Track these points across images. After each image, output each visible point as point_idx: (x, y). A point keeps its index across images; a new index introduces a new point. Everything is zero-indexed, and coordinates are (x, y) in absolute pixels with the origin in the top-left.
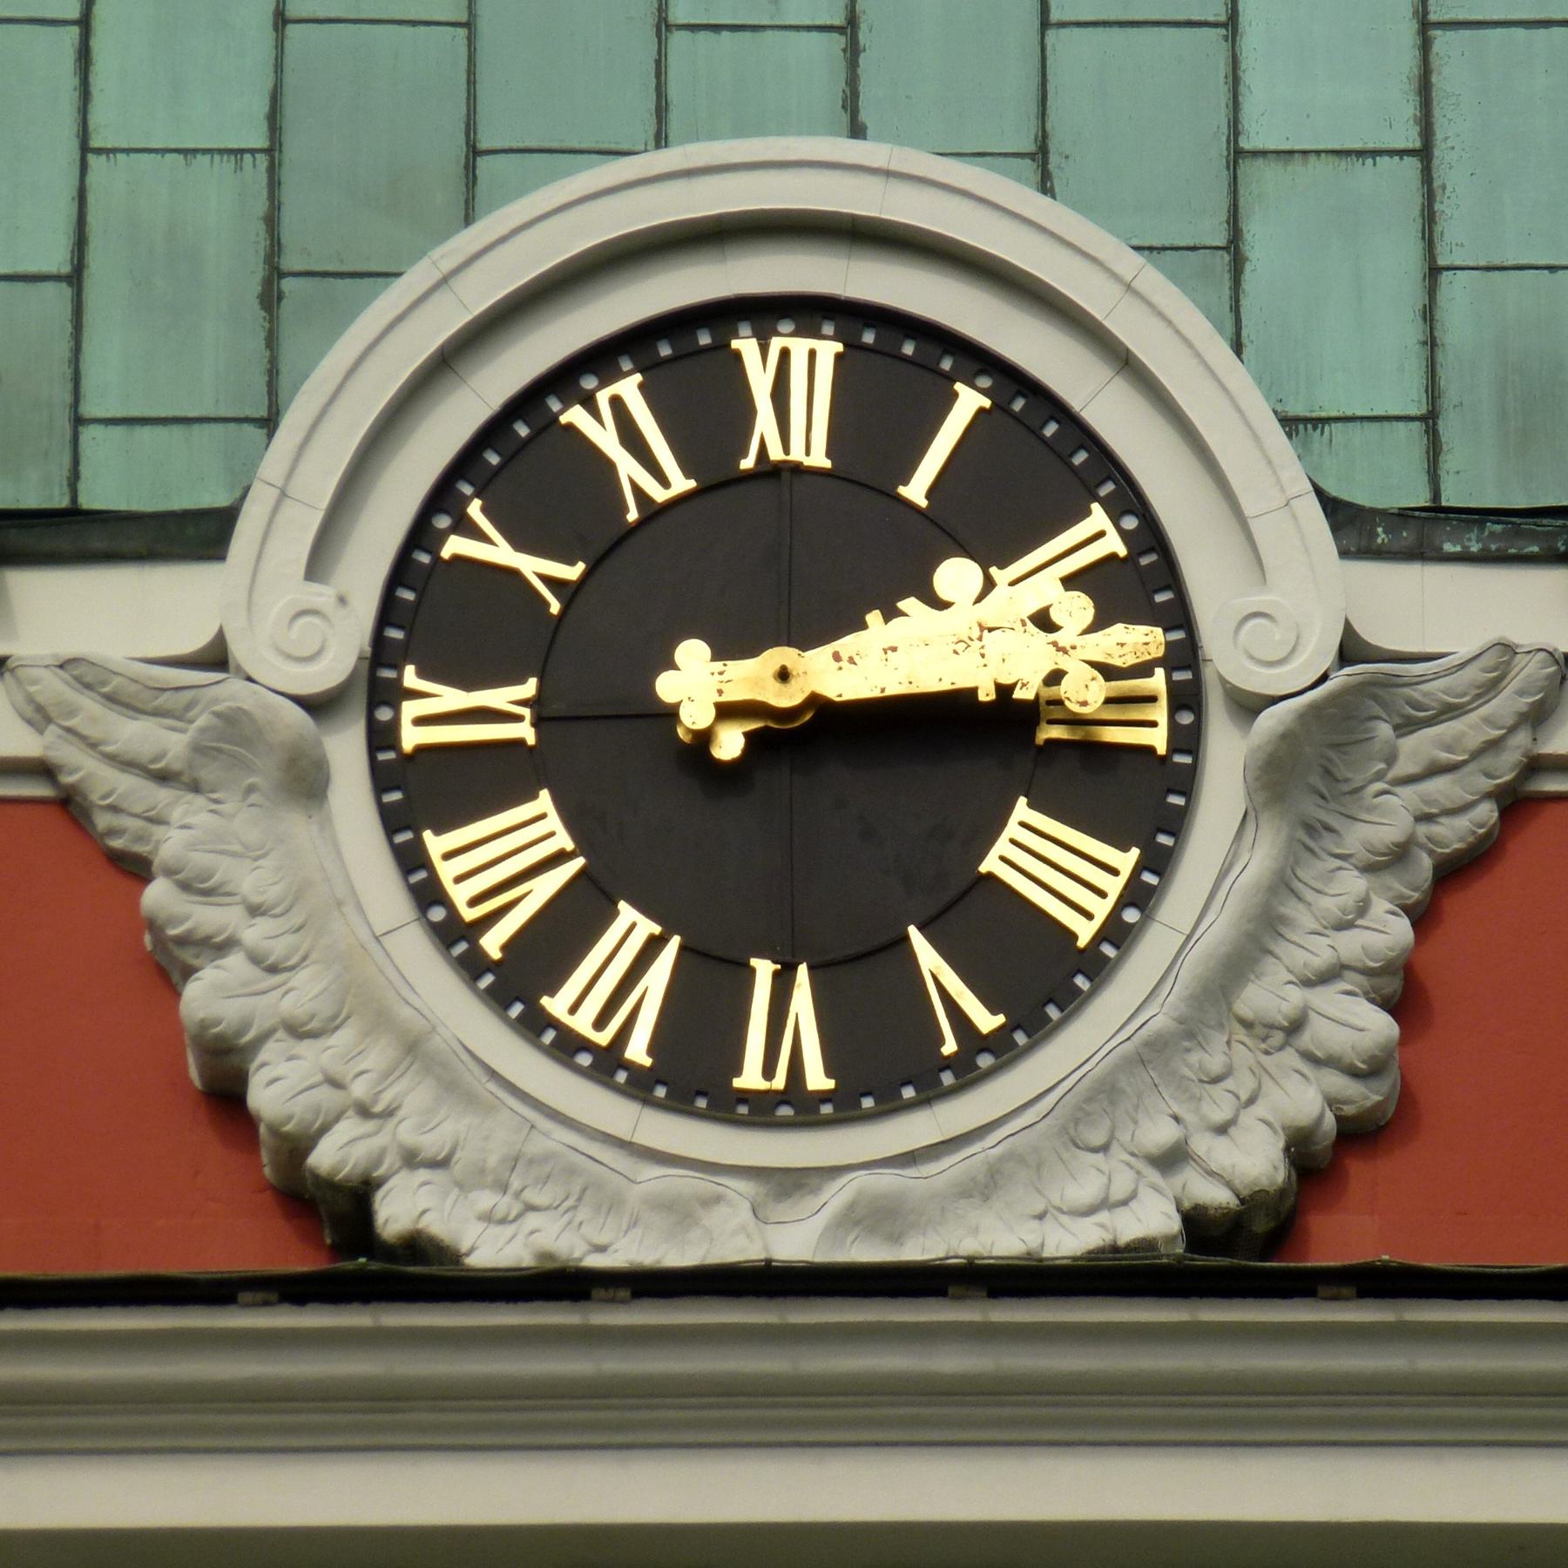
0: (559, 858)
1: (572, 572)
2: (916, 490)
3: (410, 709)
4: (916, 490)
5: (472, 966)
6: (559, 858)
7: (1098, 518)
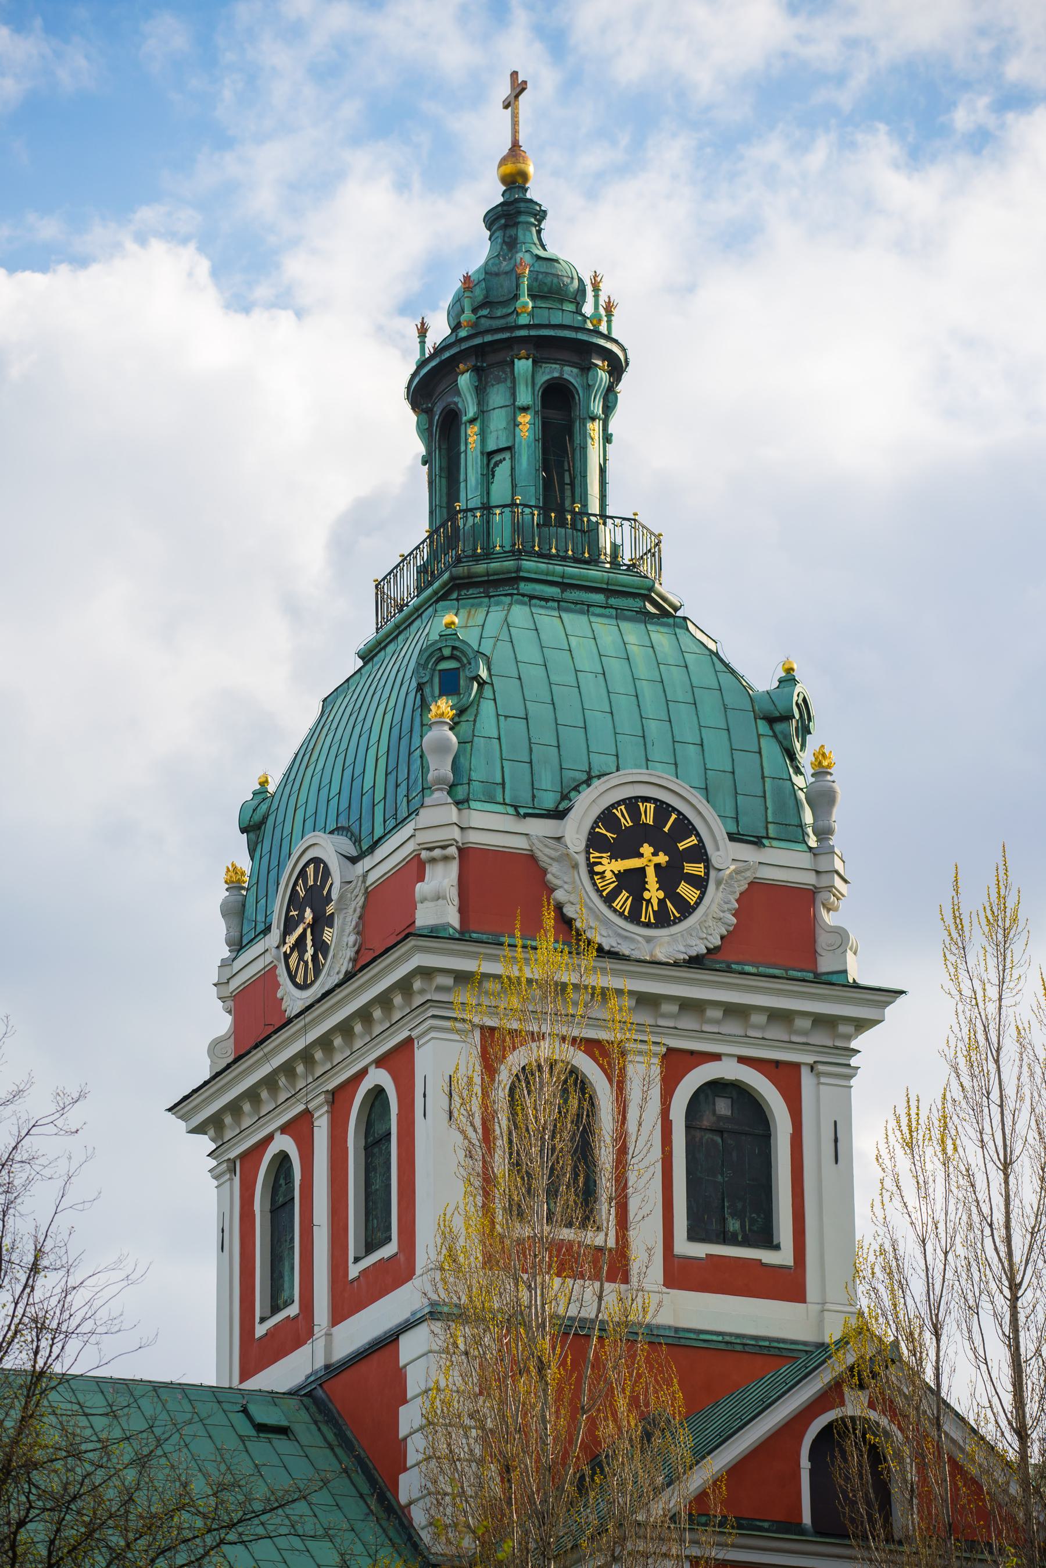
0: (614, 882)
1: (615, 836)
2: (666, 829)
3: (591, 856)
4: (666, 829)
5: (601, 896)
6: (614, 882)
7: (693, 837)
